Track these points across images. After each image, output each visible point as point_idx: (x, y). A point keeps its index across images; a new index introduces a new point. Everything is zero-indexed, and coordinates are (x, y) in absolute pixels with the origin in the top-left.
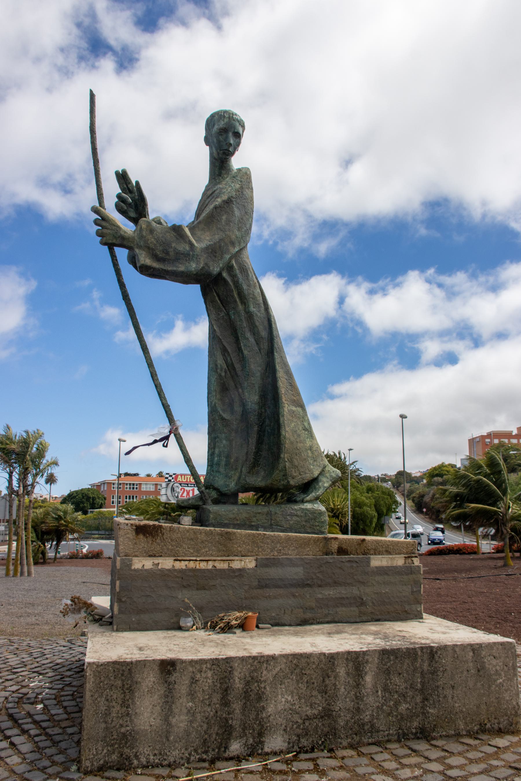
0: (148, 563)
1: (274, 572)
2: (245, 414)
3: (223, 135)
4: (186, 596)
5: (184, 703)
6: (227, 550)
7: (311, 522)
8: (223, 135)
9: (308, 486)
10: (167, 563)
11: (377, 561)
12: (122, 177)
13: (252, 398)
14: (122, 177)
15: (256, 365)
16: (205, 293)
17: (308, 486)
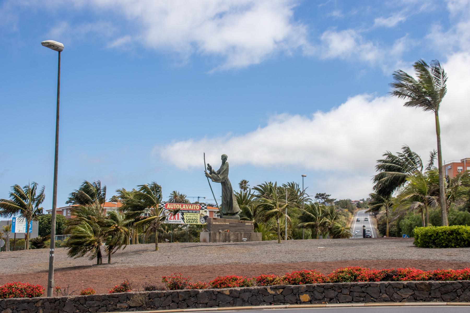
0: (215, 223)
1: (232, 225)
2: (227, 202)
3: (224, 158)
4: (220, 228)
5: (221, 237)
6: (225, 221)
7: (237, 218)
8: (224, 158)
9: (237, 213)
10: (217, 223)
11: (246, 224)
12: (208, 165)
13: (229, 200)
14: (208, 165)
15: (229, 195)
16: (222, 183)
17: (237, 213)
